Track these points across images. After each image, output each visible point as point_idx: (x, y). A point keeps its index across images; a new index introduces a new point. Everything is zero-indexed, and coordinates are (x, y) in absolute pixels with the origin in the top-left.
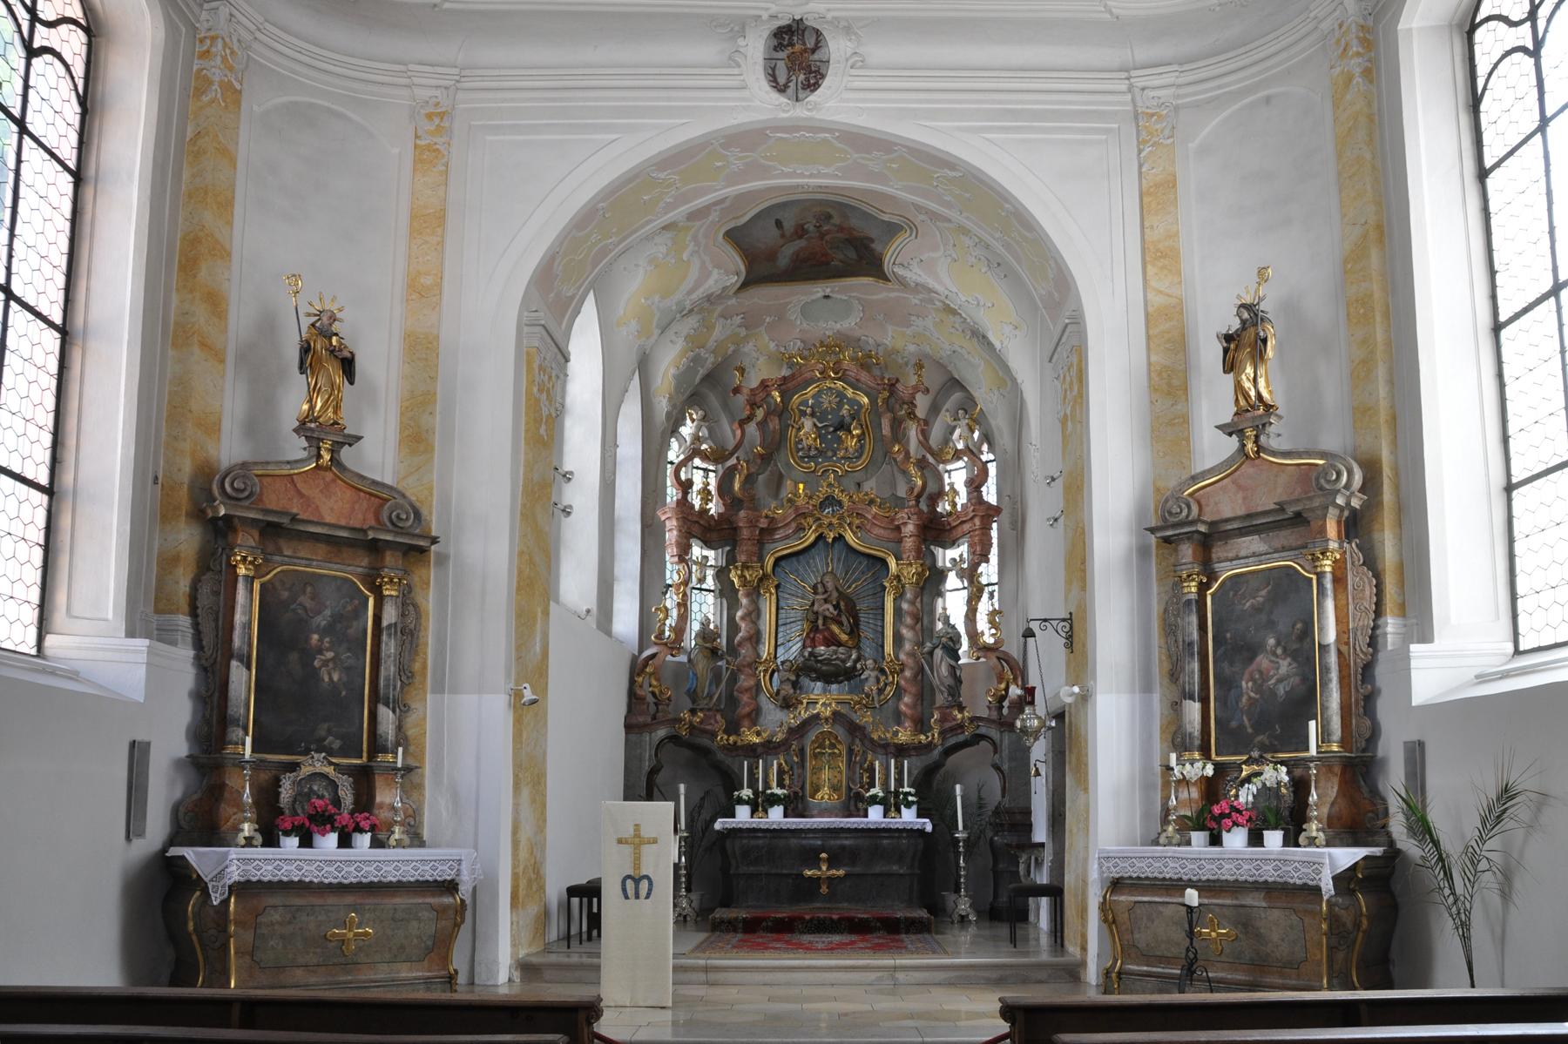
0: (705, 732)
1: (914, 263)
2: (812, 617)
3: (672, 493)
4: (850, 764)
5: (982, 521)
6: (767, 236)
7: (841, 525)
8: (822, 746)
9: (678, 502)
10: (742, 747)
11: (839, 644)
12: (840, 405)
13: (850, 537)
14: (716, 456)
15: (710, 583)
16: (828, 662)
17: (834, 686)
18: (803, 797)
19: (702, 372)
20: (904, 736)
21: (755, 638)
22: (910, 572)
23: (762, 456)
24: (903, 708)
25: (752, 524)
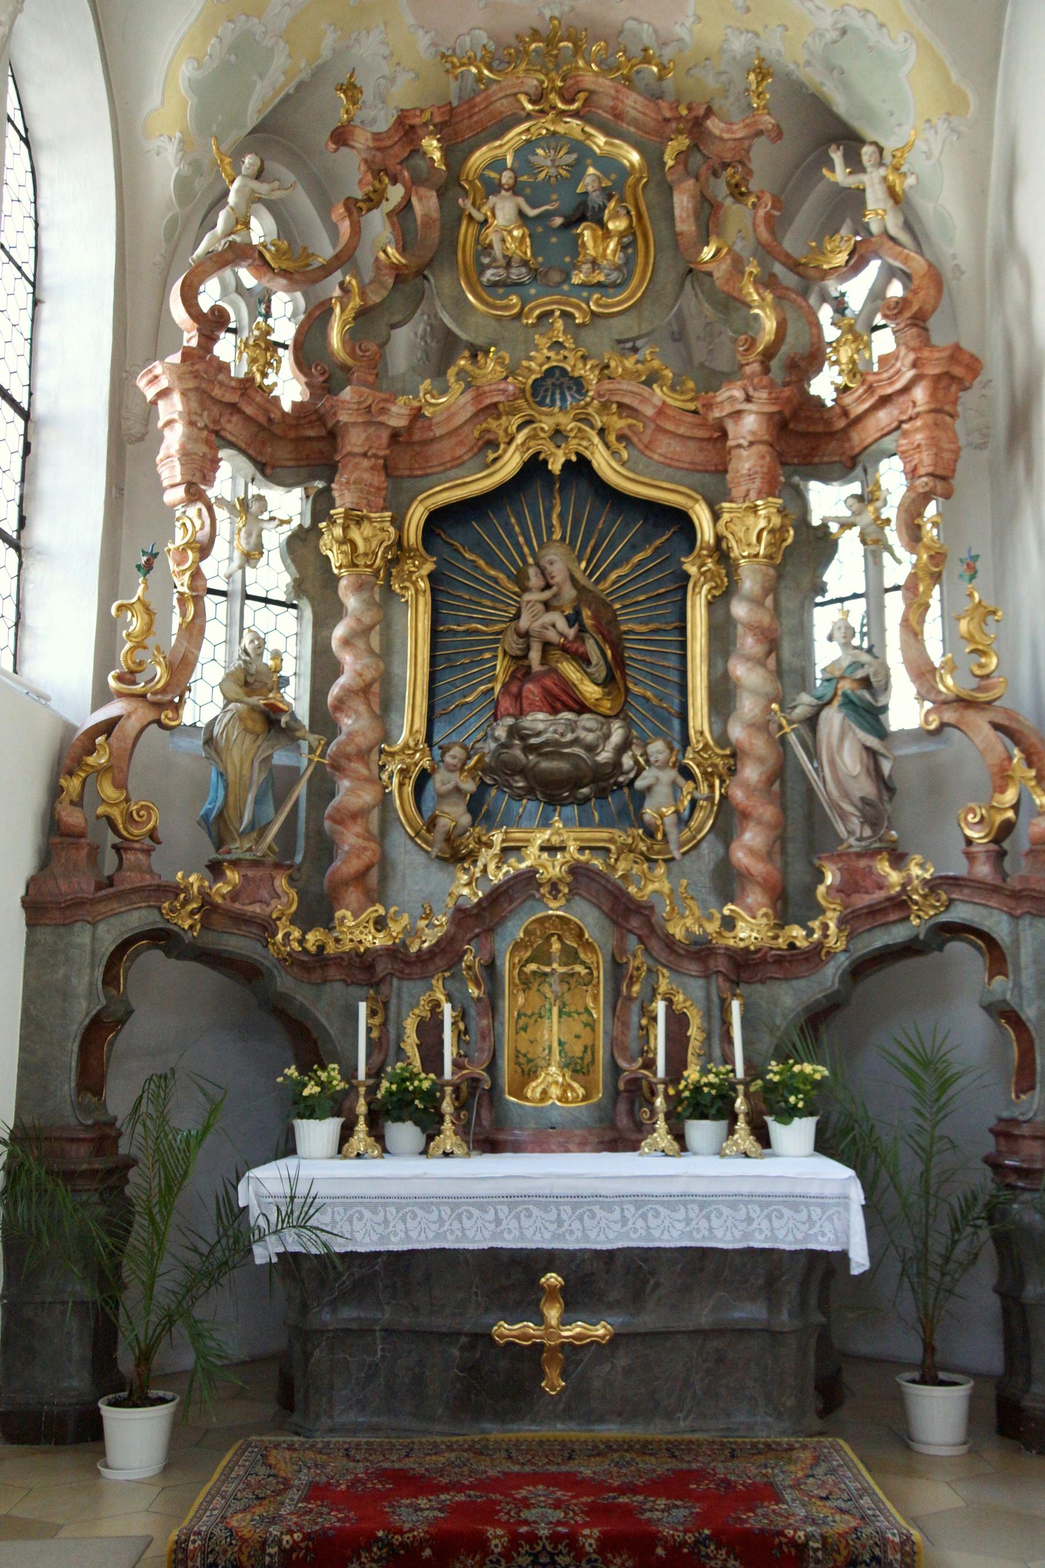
0: (241, 920)
2: (512, 644)
4: (617, 1000)
5: (933, 395)
7: (581, 434)
8: (542, 956)
10: (338, 960)
11: (581, 708)
12: (577, 170)
13: (603, 462)
14: (291, 265)
16: (552, 749)
20: (751, 930)
21: (380, 695)
22: (750, 527)
24: (740, 856)
25: (371, 416)
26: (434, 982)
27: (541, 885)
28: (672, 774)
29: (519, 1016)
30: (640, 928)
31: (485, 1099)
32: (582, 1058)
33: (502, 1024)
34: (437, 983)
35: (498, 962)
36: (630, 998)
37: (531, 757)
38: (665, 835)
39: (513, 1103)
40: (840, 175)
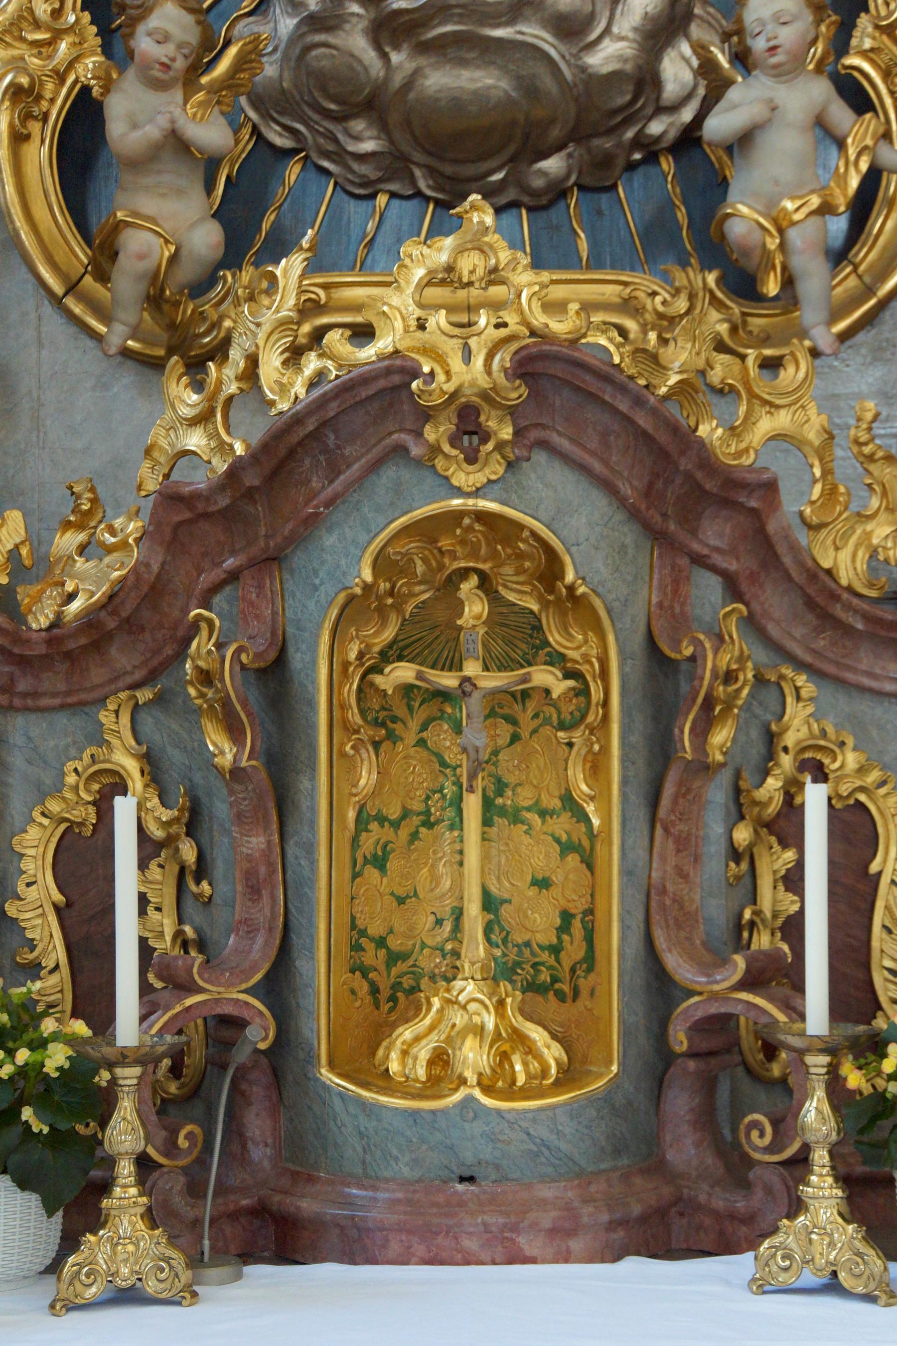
4: (662, 775)
18: (283, 1060)
26: (106, 717)
27: (426, 415)
28: (818, 91)
29: (362, 822)
30: (732, 551)
31: (257, 1091)
32: (556, 950)
33: (310, 849)
34: (114, 719)
35: (296, 660)
36: (703, 768)
37: (395, 58)
38: (789, 282)
39: (343, 1096)
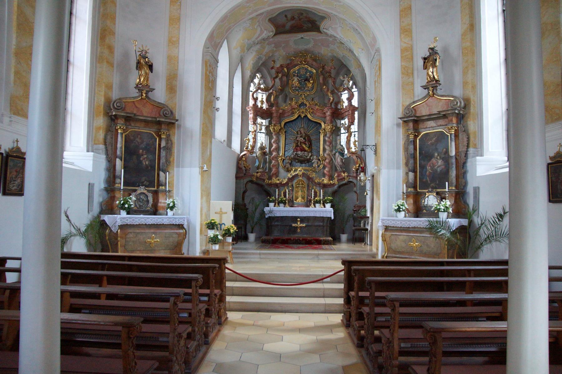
1: (330, 28)
2: (296, 142)
3: (251, 102)
6: (282, 20)
9: (253, 105)
10: (273, 184)
11: (305, 151)
12: (306, 73)
13: (309, 116)
14: (265, 90)
15: (263, 130)
16: (301, 157)
17: (304, 165)
19: (261, 62)
20: (326, 181)
21: (278, 149)
22: (329, 128)
23: (281, 90)
24: (325, 172)
28: (316, 161)
40: (341, 78)
